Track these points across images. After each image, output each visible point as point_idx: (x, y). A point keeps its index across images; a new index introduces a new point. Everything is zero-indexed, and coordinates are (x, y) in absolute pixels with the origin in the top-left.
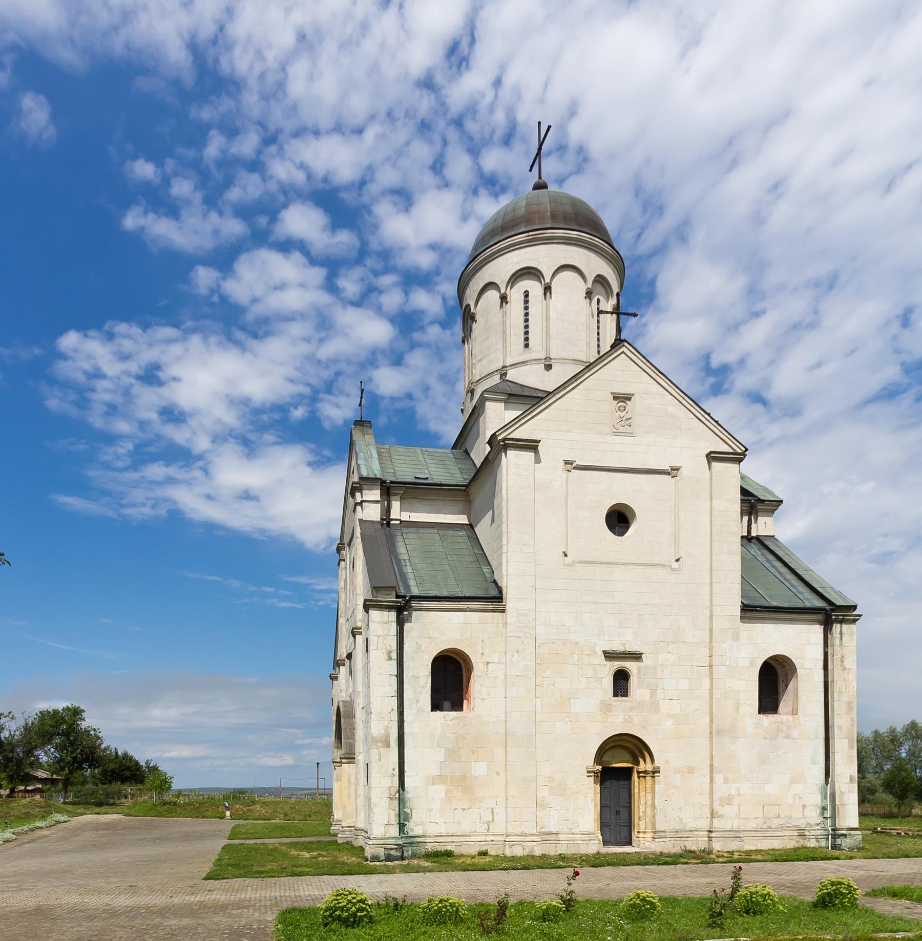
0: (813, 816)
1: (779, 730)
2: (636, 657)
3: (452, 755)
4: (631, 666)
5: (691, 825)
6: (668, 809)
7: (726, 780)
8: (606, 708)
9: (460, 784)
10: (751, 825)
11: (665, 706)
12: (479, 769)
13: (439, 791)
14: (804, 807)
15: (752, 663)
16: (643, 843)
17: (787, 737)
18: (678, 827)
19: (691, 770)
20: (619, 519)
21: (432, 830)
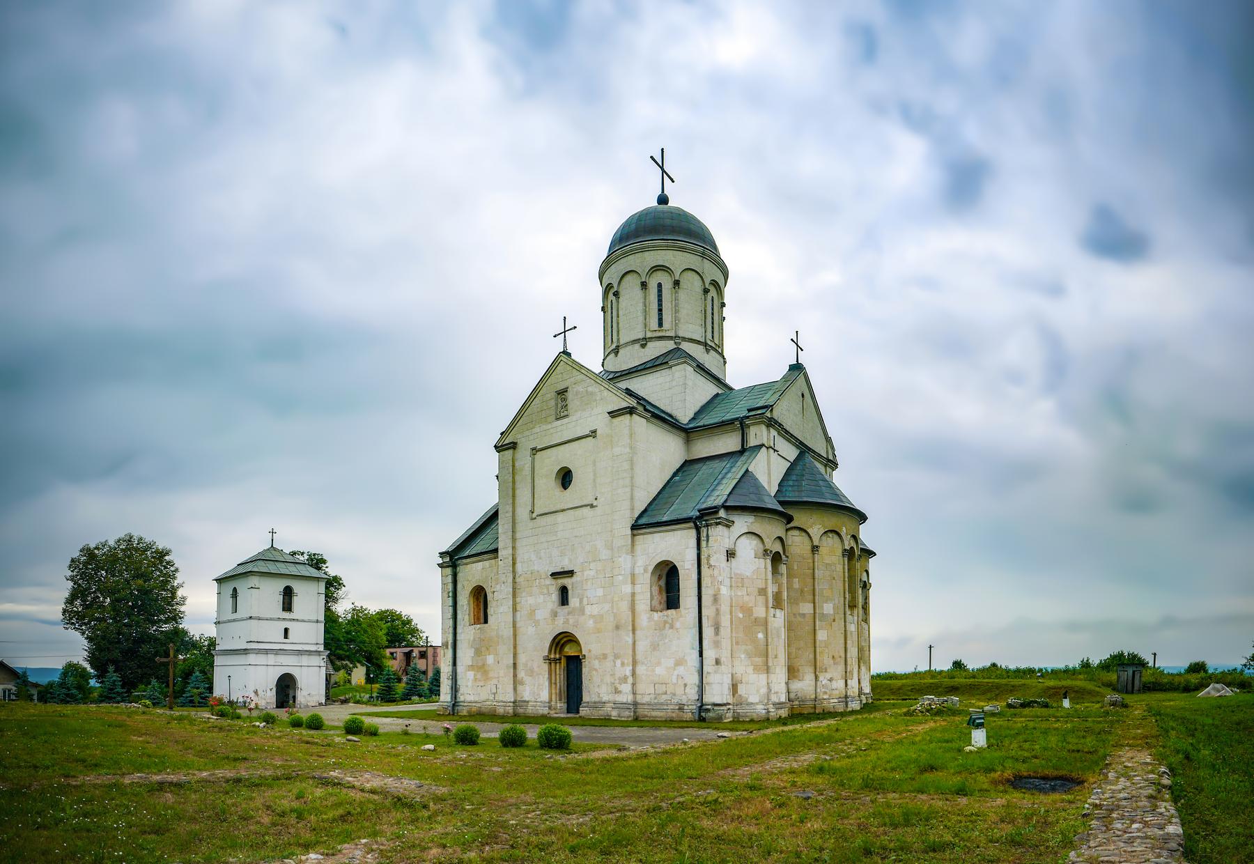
0: (692, 694)
1: (666, 622)
2: (570, 573)
3: (478, 652)
4: (567, 582)
5: (605, 698)
6: (603, 686)
7: (623, 664)
8: (555, 614)
9: (480, 668)
10: (646, 699)
11: (588, 610)
12: (490, 659)
13: (471, 674)
14: (685, 685)
15: (645, 571)
16: (583, 711)
17: (672, 627)
18: (597, 700)
19: (605, 656)
20: (565, 478)
21: (469, 698)
